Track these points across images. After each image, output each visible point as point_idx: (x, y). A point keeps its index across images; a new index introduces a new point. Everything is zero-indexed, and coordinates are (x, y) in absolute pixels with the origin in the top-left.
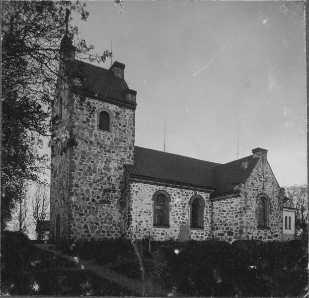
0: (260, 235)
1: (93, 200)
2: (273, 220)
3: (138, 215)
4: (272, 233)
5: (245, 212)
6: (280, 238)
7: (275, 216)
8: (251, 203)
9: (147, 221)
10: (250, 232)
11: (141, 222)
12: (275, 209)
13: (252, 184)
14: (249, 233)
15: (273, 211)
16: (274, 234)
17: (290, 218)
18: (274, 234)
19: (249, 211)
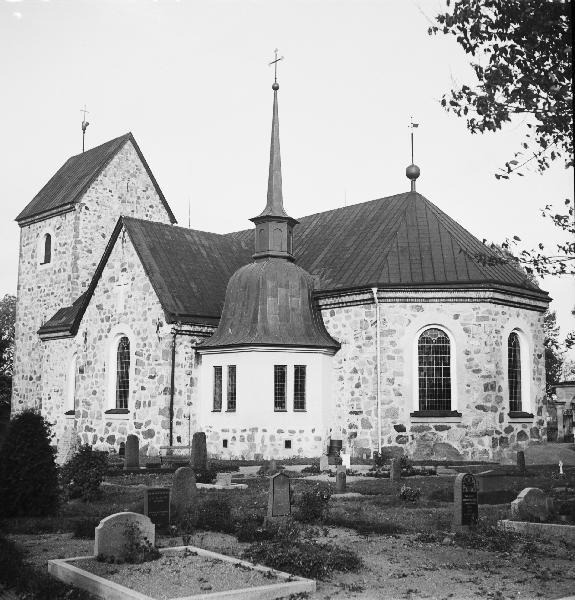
0: (111, 433)
1: (31, 379)
2: (143, 388)
3: (47, 397)
4: (138, 426)
5: (83, 378)
6: (158, 439)
7: (146, 379)
8: (95, 356)
9: (58, 407)
10: (90, 426)
11: (52, 408)
12: (148, 358)
13: (99, 307)
14: (88, 429)
15: (142, 364)
16: (143, 429)
17: (300, 371)
18: (143, 429)
19: (90, 374)
